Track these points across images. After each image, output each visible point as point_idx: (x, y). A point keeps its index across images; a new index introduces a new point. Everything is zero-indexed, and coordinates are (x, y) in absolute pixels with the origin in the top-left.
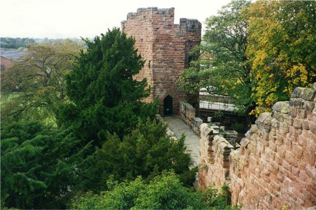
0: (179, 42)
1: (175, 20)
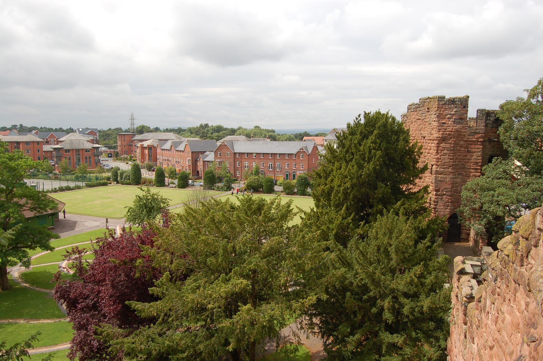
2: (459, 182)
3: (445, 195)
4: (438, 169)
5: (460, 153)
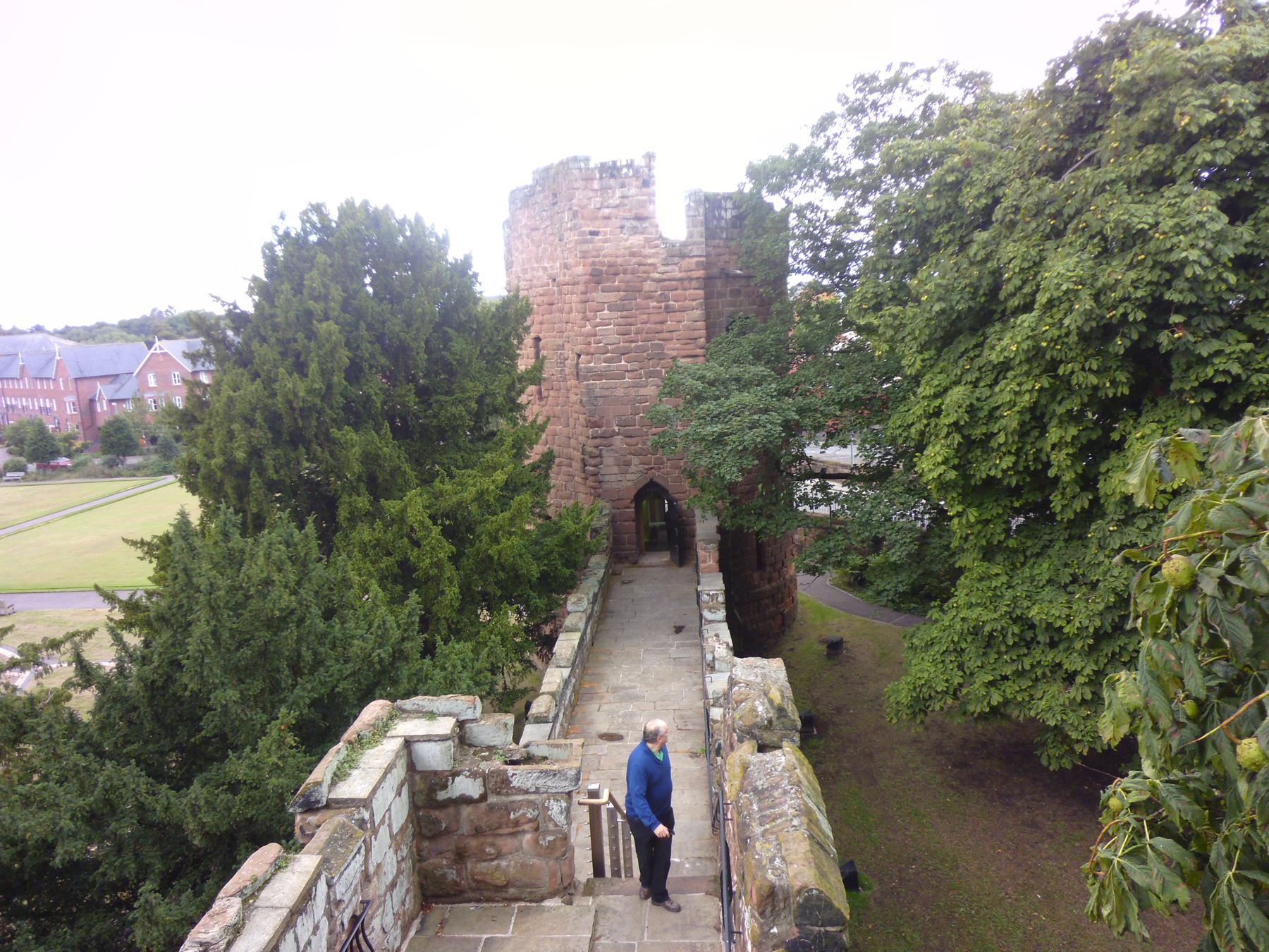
1: (657, 199)
5: (645, 317)
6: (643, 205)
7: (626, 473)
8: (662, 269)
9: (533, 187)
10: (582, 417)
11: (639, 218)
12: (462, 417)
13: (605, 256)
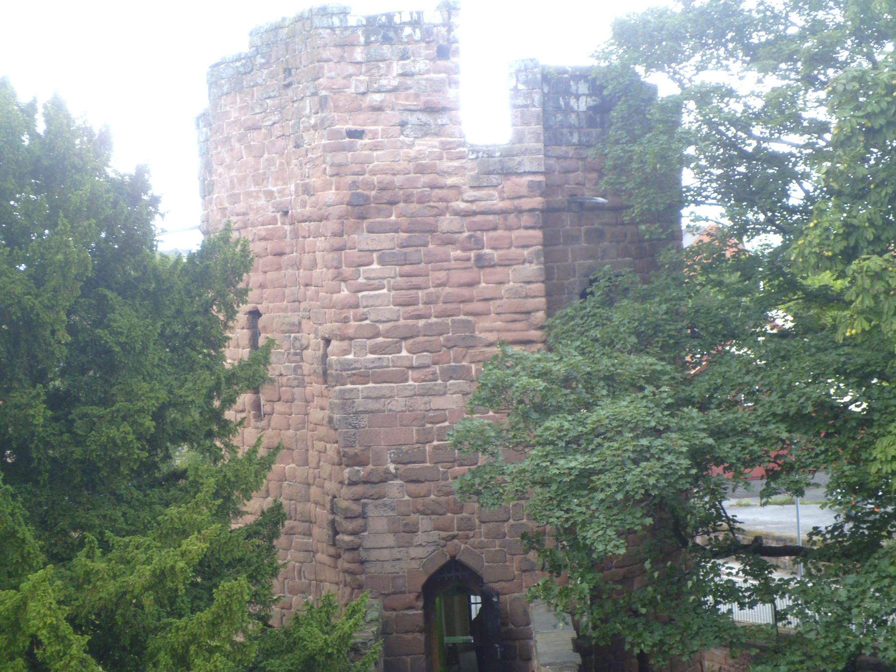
0: (503, 212)
2: (452, 411)
3: (395, 477)
4: (351, 357)
5: (442, 275)
6: (438, 87)
7: (409, 544)
8: (470, 194)
9: (250, 58)
10: (332, 449)
11: (432, 110)
12: (126, 445)
13: (373, 173)
